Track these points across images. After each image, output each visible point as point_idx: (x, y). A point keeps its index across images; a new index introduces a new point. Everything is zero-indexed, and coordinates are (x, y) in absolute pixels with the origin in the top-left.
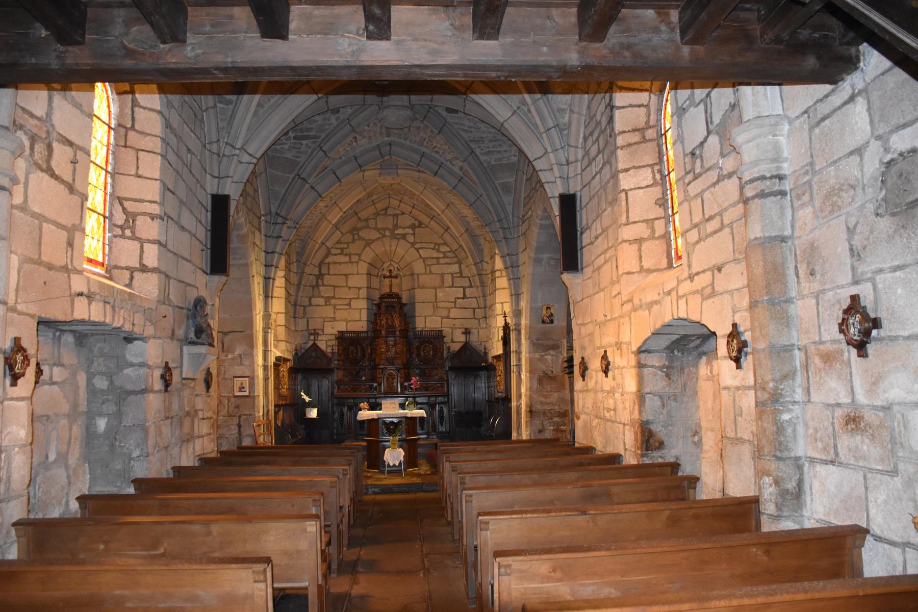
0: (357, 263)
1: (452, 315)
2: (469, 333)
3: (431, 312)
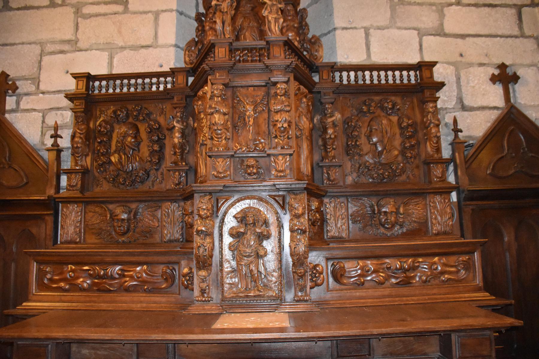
1: (449, 28)
2: (515, 78)
3: (383, 16)
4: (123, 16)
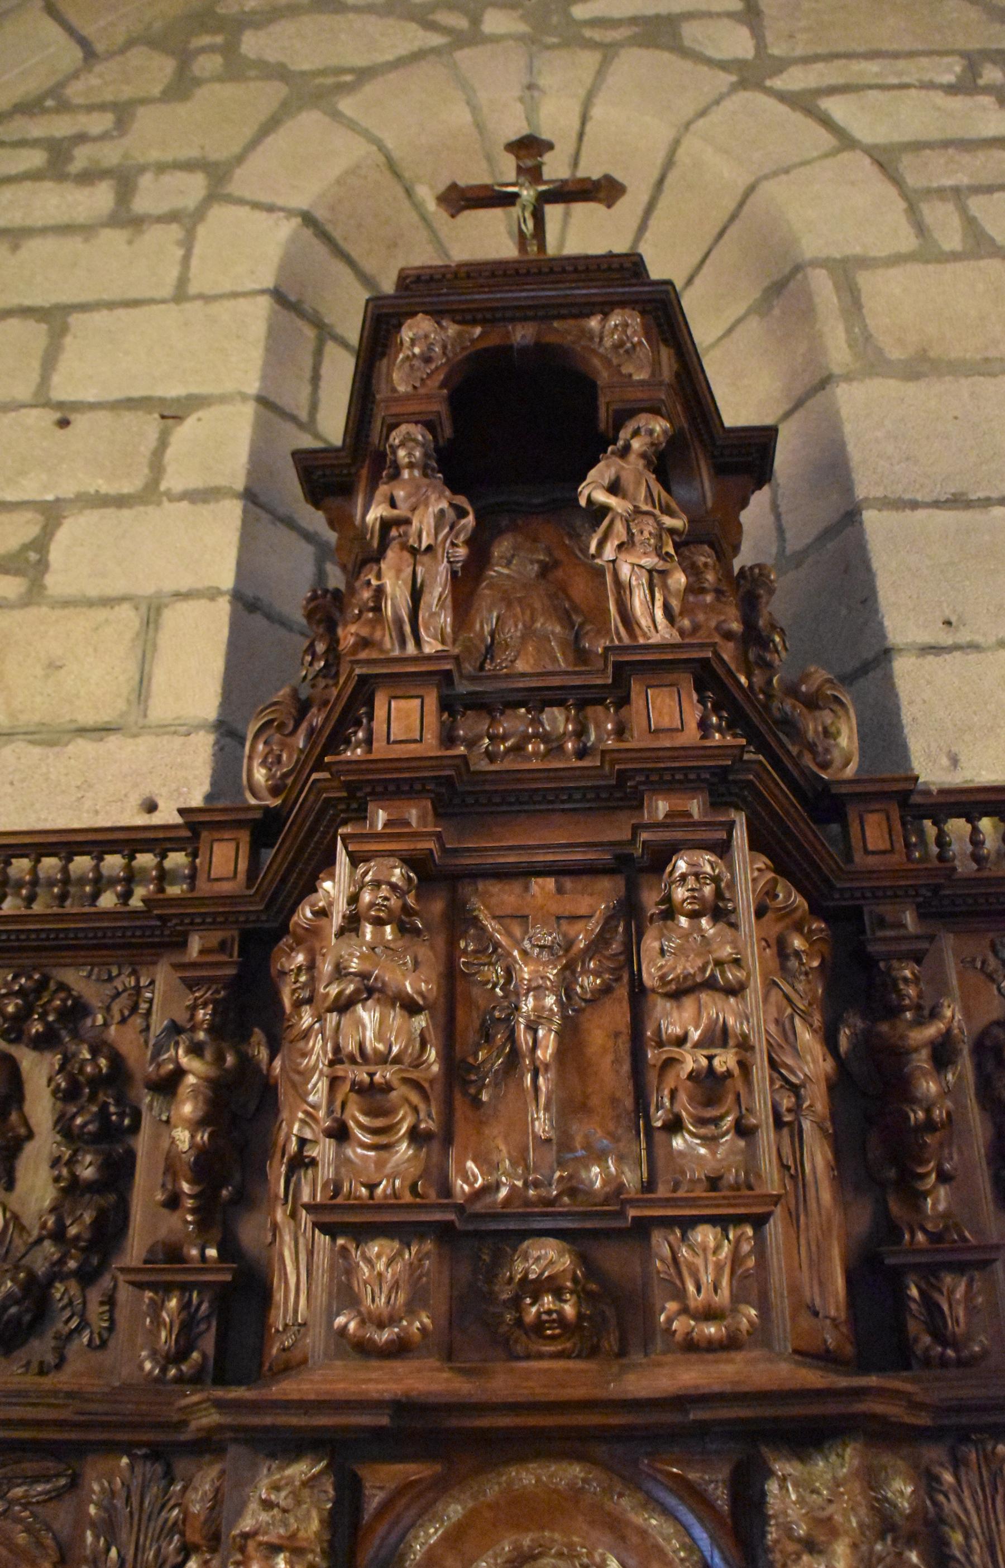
0: (188, 221)
4: (18, 615)
